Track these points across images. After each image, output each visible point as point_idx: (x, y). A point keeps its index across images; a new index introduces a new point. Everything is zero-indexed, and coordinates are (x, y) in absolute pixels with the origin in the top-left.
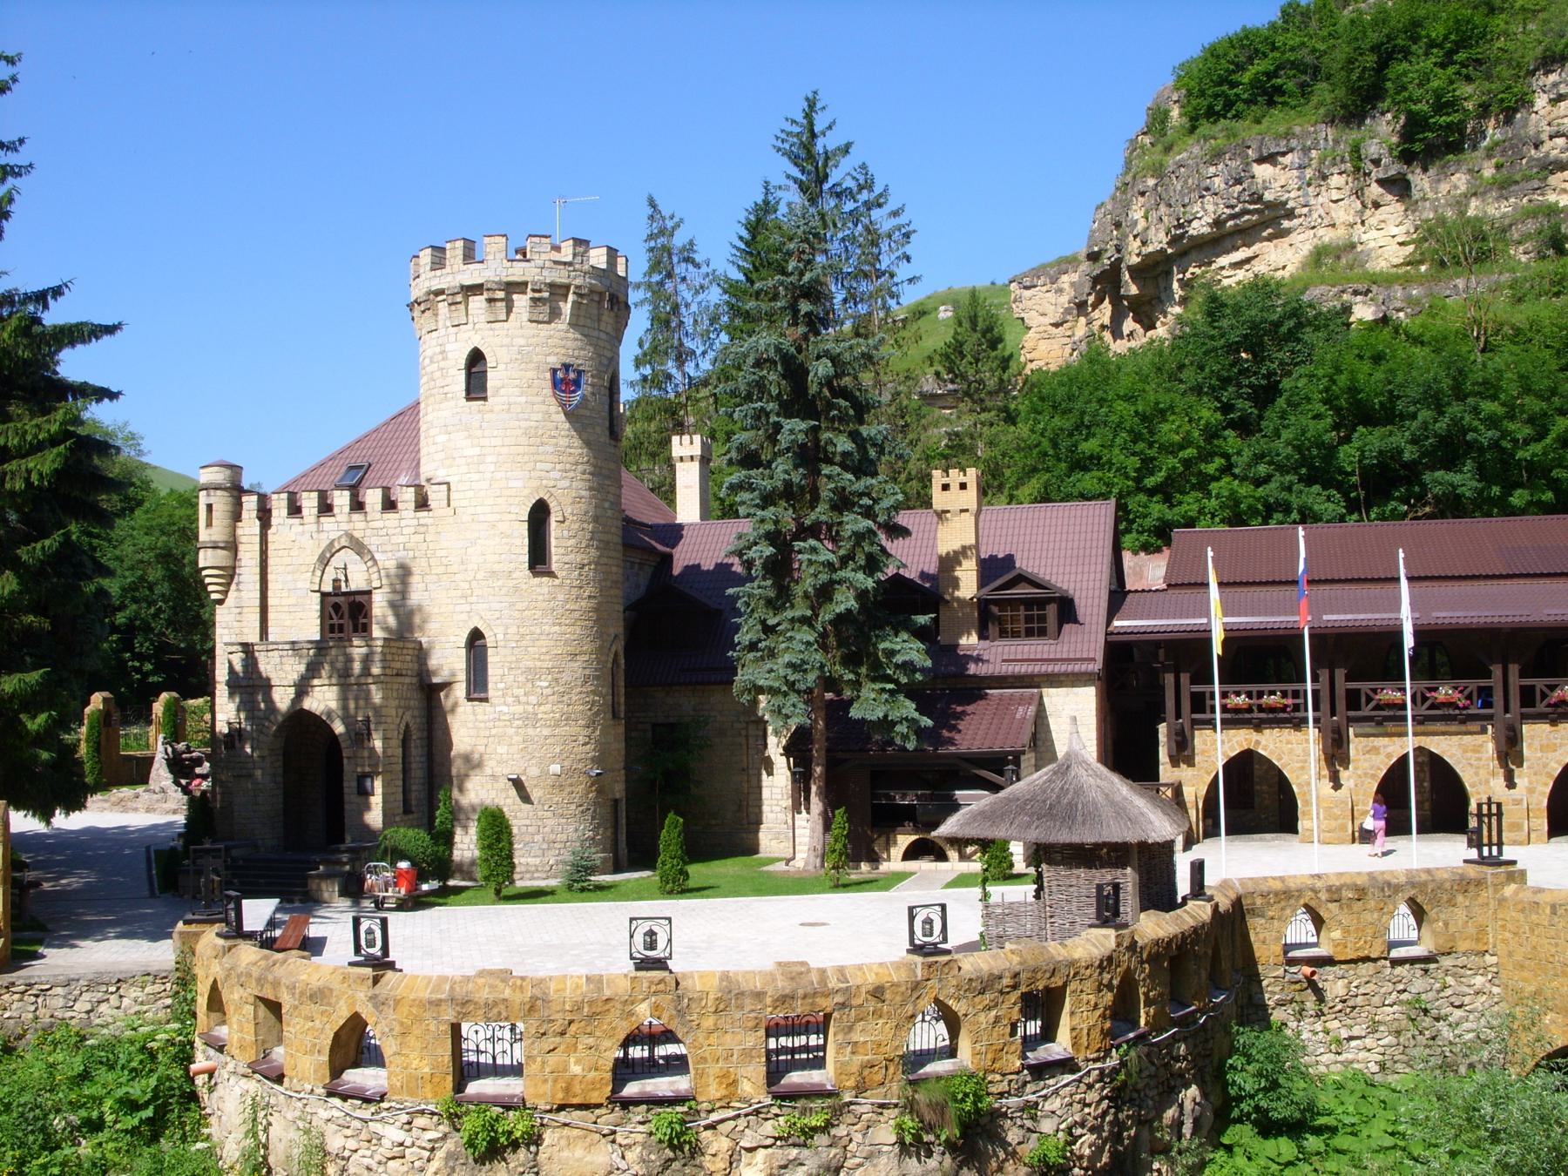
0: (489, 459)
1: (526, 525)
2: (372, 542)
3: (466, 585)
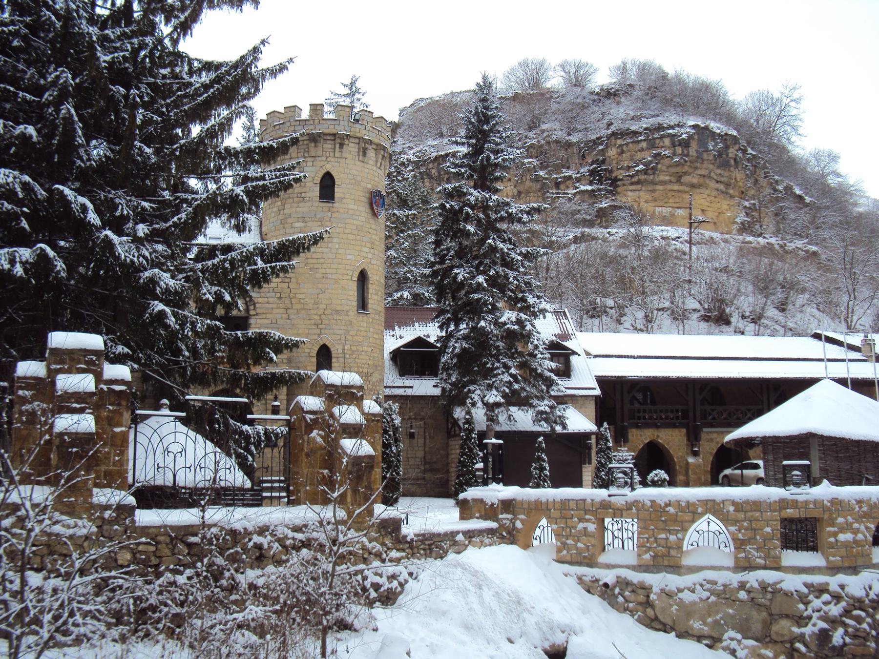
0: (335, 240)
1: (356, 284)
3: (317, 317)
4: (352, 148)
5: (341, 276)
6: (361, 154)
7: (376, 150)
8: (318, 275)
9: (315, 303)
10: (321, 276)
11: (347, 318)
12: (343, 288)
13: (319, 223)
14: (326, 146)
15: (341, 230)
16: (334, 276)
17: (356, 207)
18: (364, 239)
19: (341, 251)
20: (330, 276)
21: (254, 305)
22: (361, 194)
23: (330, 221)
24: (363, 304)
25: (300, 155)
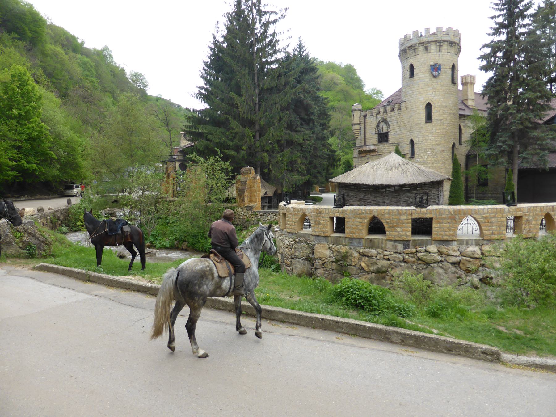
2: (388, 119)
4: (421, 48)
9: (409, 122)
12: (419, 113)
24: (429, 118)
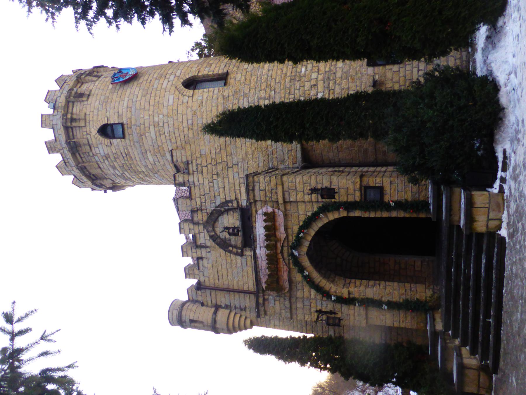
0: (156, 119)
2: (209, 207)
4: (77, 109)
5: (189, 109)
6: (80, 99)
7: (83, 83)
8: (191, 135)
10: (191, 131)
11: (231, 98)
13: (143, 137)
14: (79, 137)
15: (147, 113)
16: (190, 117)
17: (126, 99)
18: (155, 86)
19: (165, 112)
20: (190, 122)
21: (227, 202)
22: (115, 95)
23: (139, 126)
25: (94, 160)
